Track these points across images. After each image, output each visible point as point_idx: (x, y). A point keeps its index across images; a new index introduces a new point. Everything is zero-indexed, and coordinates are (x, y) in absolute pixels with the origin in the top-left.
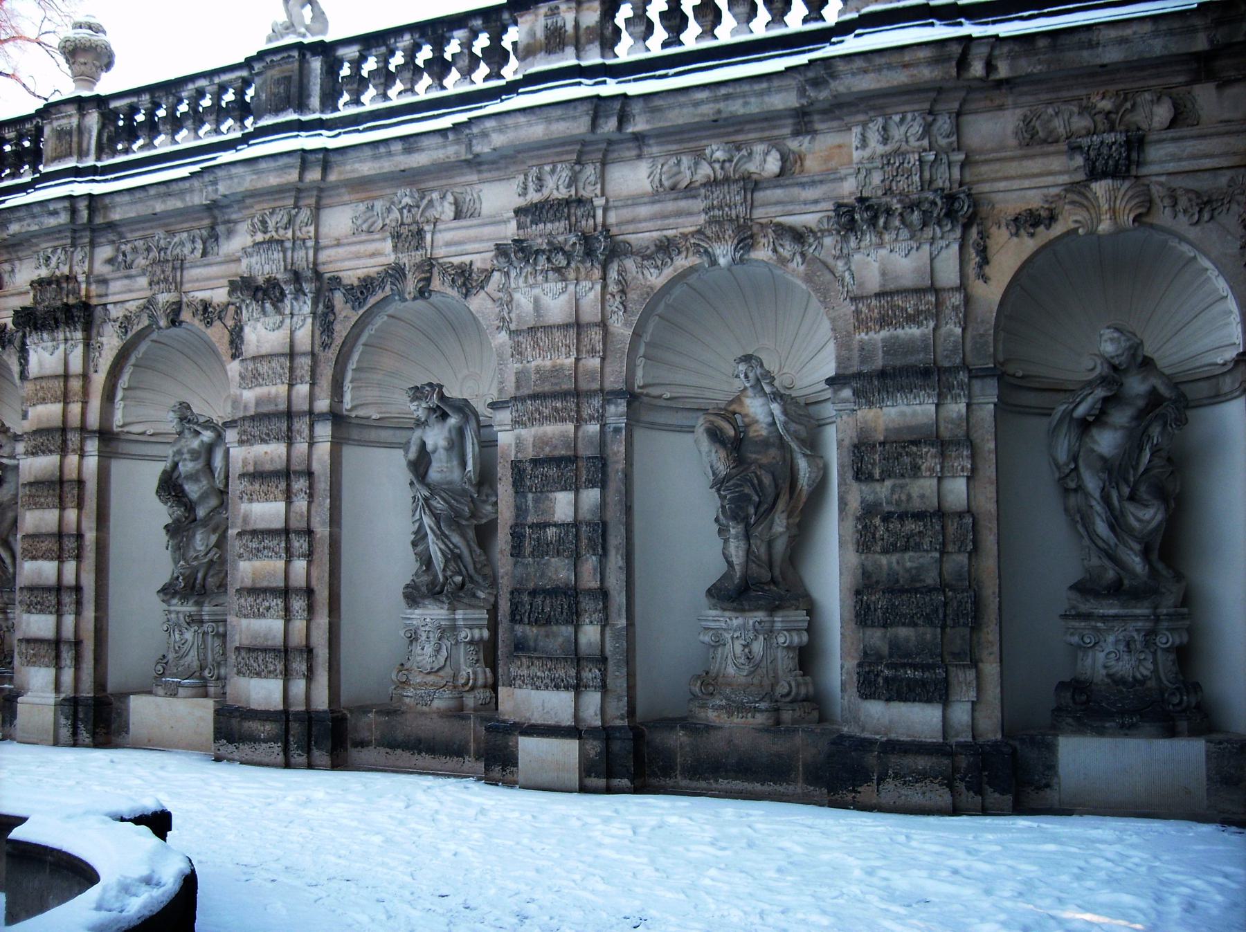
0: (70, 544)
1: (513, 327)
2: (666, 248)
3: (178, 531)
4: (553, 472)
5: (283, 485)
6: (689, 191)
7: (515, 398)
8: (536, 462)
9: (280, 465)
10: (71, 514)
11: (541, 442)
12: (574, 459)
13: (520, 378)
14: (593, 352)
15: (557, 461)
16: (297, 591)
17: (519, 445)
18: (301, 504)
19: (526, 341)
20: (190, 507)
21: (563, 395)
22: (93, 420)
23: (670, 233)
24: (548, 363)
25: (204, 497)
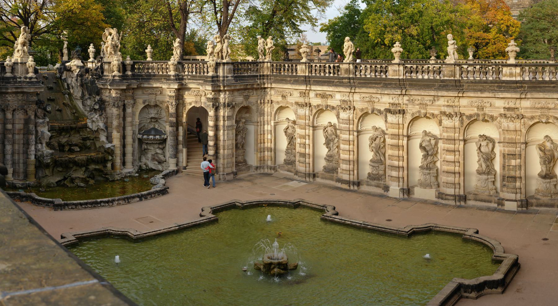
0: (401, 158)
1: (503, 128)
2: (532, 118)
3: (425, 157)
4: (511, 156)
5: (454, 153)
6: (538, 109)
7: (503, 142)
8: (508, 154)
9: (453, 149)
10: (401, 152)
11: (509, 151)
12: (515, 155)
13: (504, 138)
14: (519, 135)
15: (512, 155)
16: (457, 173)
17: (504, 150)
18: (457, 157)
19: (506, 132)
20: (427, 152)
21: (514, 143)
22: (405, 133)
23: (534, 115)
24: (510, 137)
25: (430, 150)
